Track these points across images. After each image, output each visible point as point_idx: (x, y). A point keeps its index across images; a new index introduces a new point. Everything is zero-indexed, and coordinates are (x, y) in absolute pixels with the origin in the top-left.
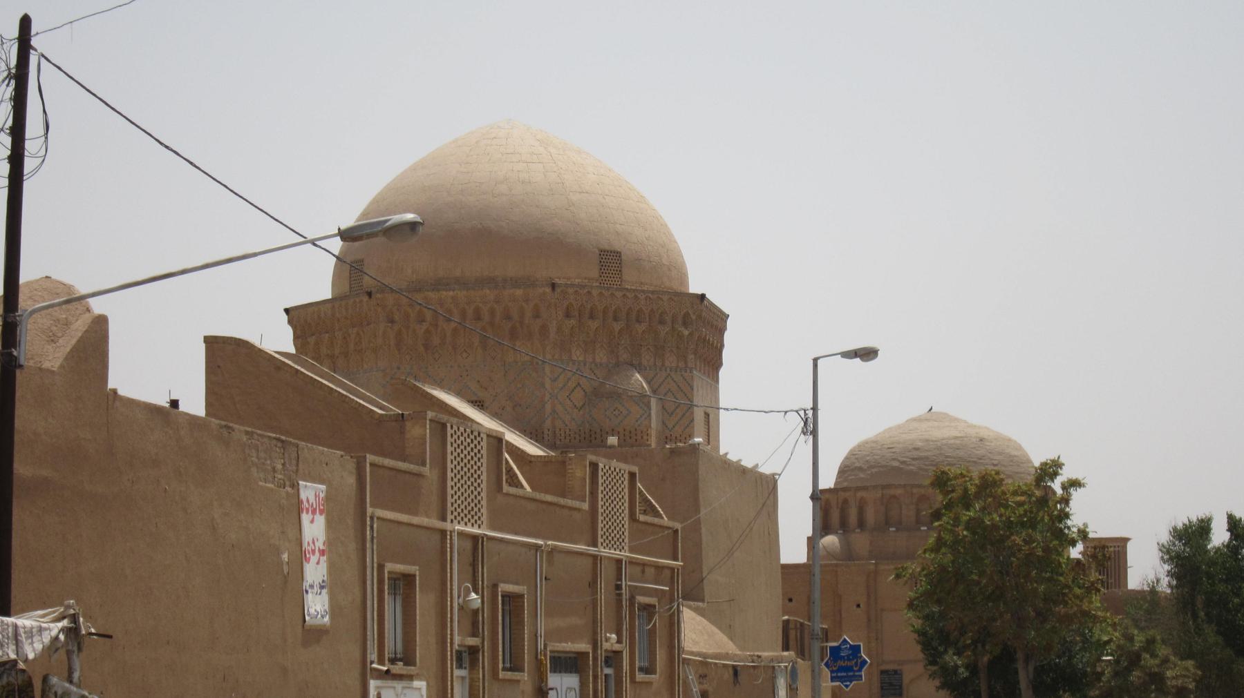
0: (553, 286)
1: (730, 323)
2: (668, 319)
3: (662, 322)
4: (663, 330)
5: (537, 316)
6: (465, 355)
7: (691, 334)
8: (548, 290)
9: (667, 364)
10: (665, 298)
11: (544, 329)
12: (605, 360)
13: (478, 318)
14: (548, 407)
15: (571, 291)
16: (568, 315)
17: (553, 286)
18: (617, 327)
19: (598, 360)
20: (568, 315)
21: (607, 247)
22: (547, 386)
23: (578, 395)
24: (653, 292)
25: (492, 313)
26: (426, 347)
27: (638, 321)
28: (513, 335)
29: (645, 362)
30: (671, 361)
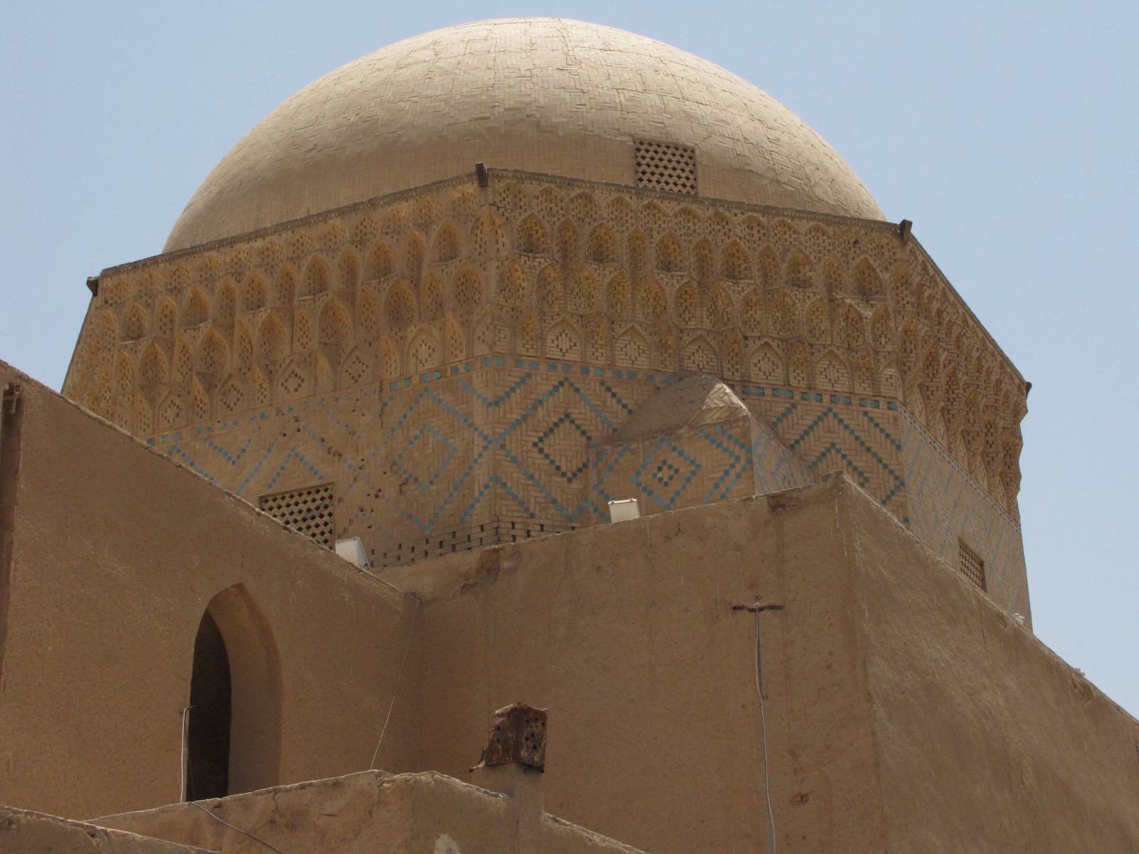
0: (482, 176)
1: (1032, 400)
2: (816, 276)
3: (801, 284)
4: (803, 304)
5: (449, 250)
6: (292, 383)
7: (882, 319)
8: (471, 188)
9: (822, 383)
10: (804, 226)
11: (466, 288)
12: (643, 363)
13: (319, 283)
14: (481, 474)
15: (532, 188)
16: (530, 247)
17: (482, 176)
18: (671, 285)
19: (622, 363)
20: (530, 247)
21: (654, 134)
22: (478, 419)
23: (566, 446)
24: (766, 210)
25: (350, 270)
26: (209, 380)
27: (732, 274)
28: (398, 314)
29: (756, 376)
30: (832, 378)
